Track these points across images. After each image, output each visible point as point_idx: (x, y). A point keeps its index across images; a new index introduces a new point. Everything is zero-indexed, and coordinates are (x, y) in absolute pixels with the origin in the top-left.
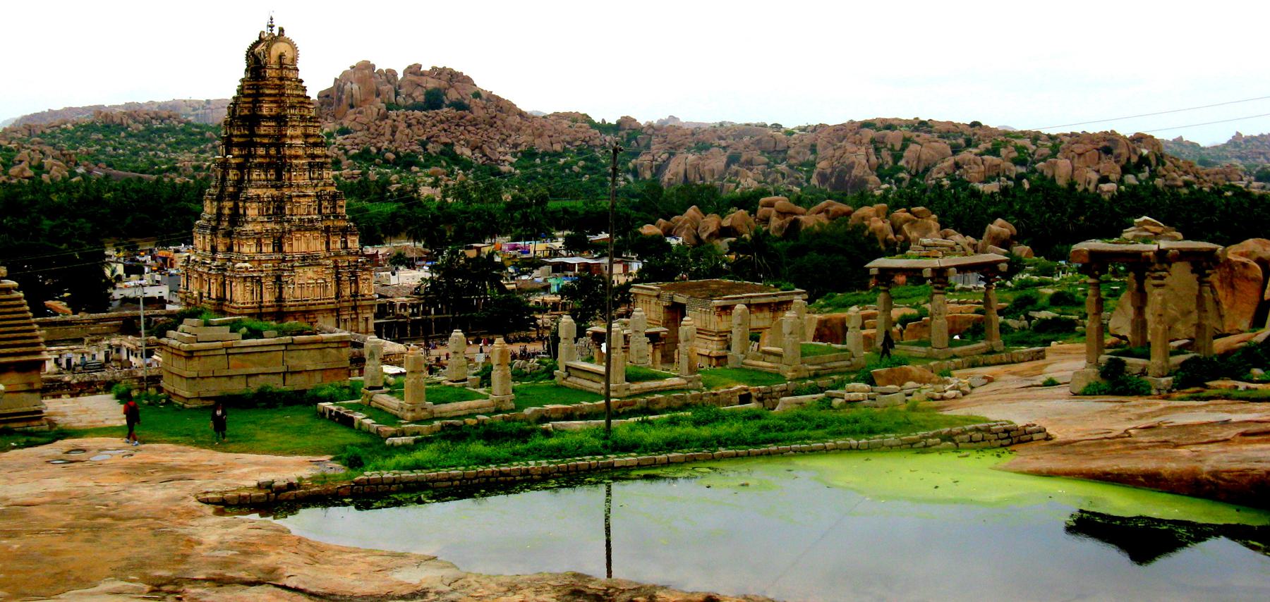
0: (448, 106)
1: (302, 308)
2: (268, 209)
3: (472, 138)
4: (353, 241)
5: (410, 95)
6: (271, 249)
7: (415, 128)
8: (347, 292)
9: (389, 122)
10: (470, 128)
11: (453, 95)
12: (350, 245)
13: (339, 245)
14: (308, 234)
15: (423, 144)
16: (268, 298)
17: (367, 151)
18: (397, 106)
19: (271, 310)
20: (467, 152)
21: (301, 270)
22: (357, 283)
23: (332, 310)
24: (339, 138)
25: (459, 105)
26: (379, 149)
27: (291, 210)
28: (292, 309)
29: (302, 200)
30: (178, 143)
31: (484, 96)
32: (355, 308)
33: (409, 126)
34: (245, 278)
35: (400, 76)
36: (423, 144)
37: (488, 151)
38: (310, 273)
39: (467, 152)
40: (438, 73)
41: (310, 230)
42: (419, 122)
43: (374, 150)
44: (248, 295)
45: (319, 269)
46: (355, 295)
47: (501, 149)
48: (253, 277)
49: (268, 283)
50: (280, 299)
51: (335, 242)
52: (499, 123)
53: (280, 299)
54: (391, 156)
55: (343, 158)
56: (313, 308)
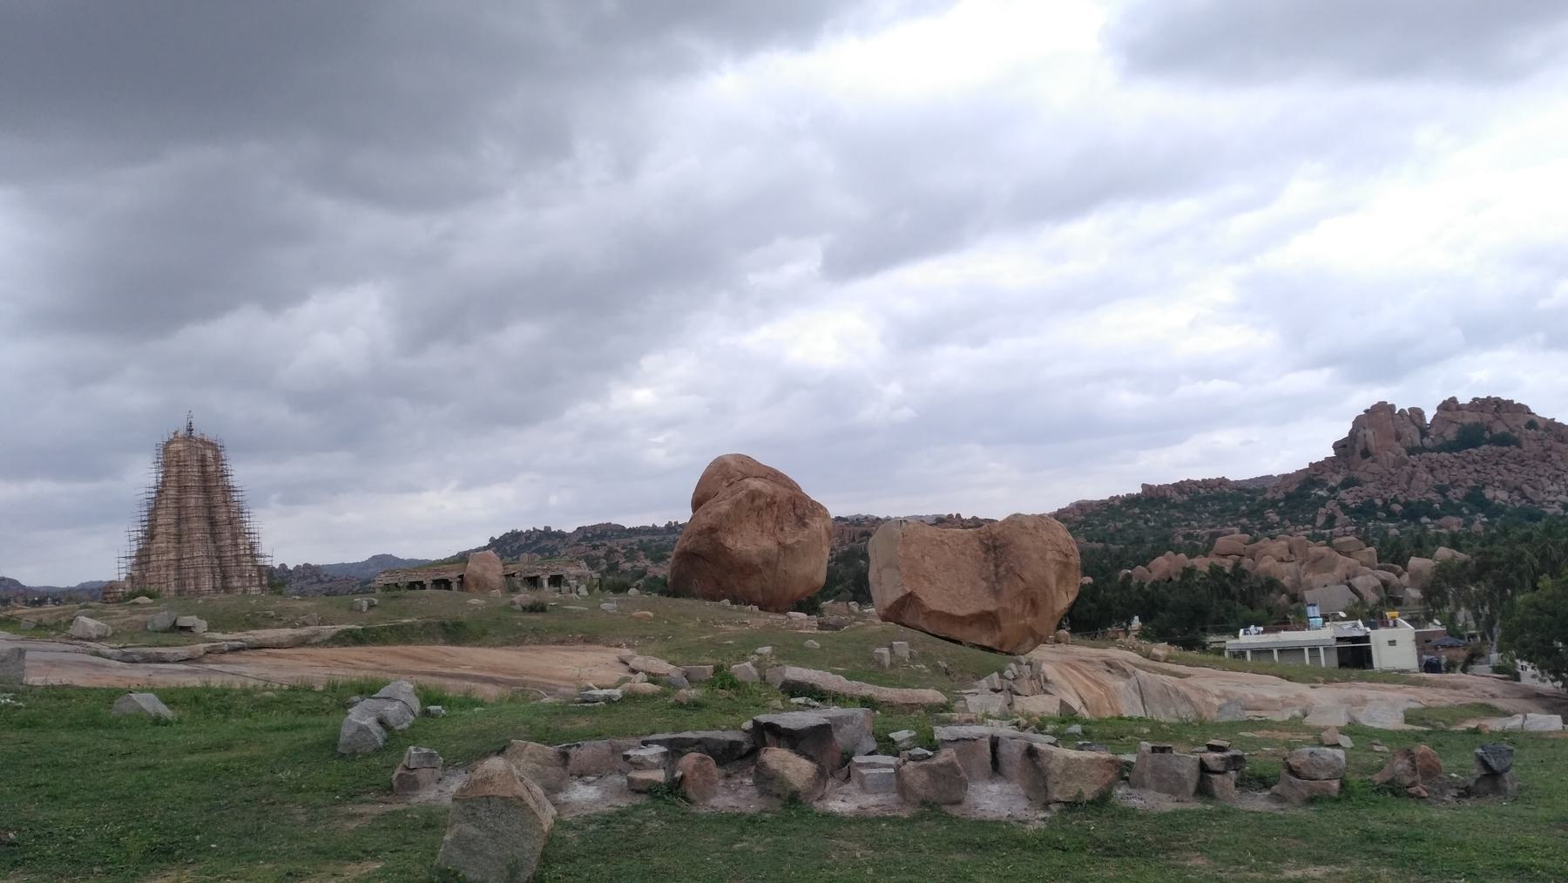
0: (1489, 442)
3: (1510, 478)
5: (1441, 435)
7: (1438, 473)
9: (1408, 468)
10: (1512, 466)
11: (1499, 428)
15: (1442, 490)
17: (1371, 504)
18: (1423, 449)
20: (1502, 495)
24: (1342, 494)
25: (1504, 440)
26: (1385, 502)
30: (1222, 511)
31: (1541, 425)
33: (1432, 470)
35: (1429, 418)
36: (1442, 490)
37: (1528, 490)
39: (1502, 495)
40: (1479, 405)
42: (1443, 466)
43: (1379, 502)
47: (1555, 487)
52: (1555, 456)
54: (1397, 508)
55: (1342, 517)
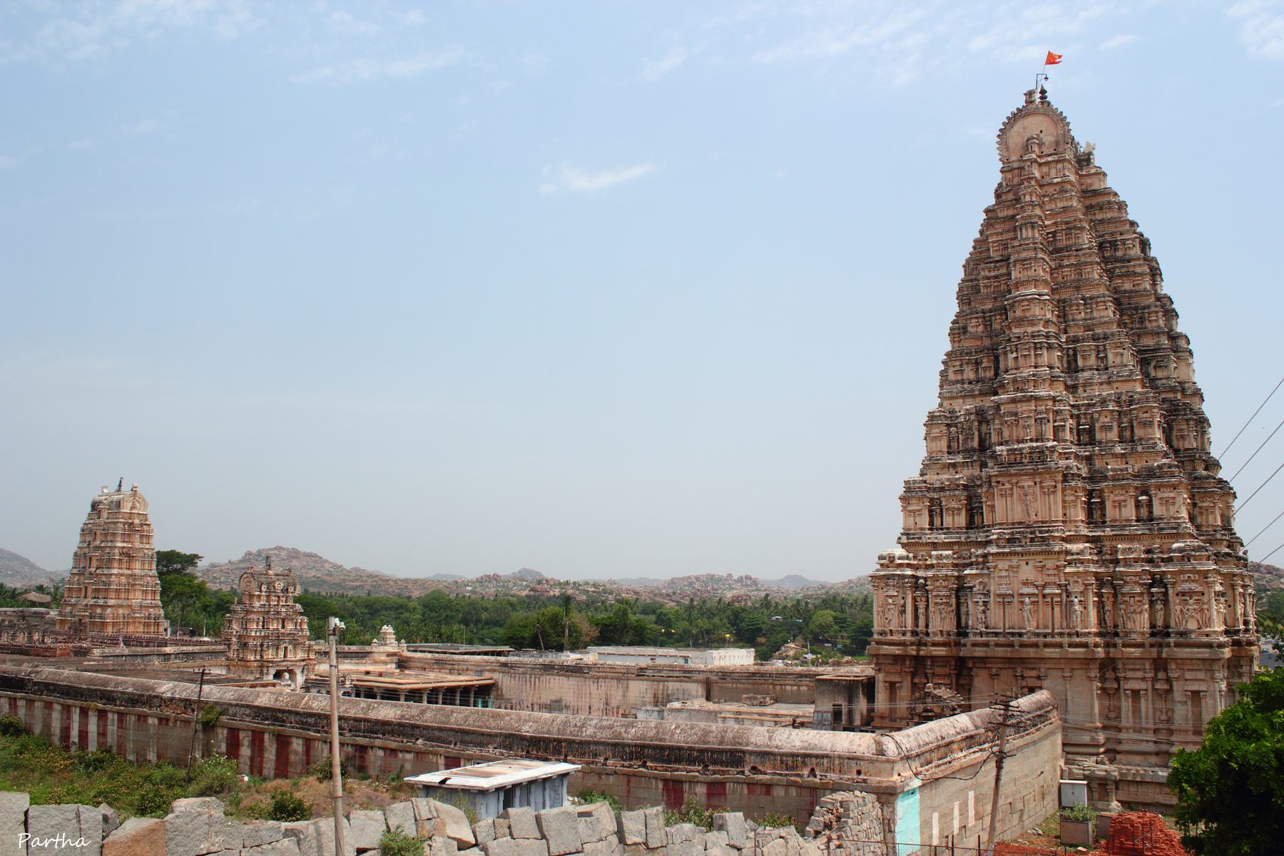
1: (1000, 652)
2: (969, 437)
4: (1166, 502)
6: (961, 520)
8: (1141, 623)
12: (1158, 510)
13: (1130, 512)
14: (1026, 483)
16: (940, 623)
19: (941, 651)
21: (1003, 564)
22: (1166, 602)
23: (1087, 662)
27: (1000, 433)
28: (979, 652)
29: (1022, 408)
32: (1160, 664)
34: (888, 577)
38: (1027, 572)
41: (1034, 474)
44: (893, 615)
45: (1050, 563)
46: (1160, 633)
48: (904, 577)
49: (940, 592)
50: (962, 631)
51: (1119, 505)
53: (962, 631)
56: (1031, 652)
